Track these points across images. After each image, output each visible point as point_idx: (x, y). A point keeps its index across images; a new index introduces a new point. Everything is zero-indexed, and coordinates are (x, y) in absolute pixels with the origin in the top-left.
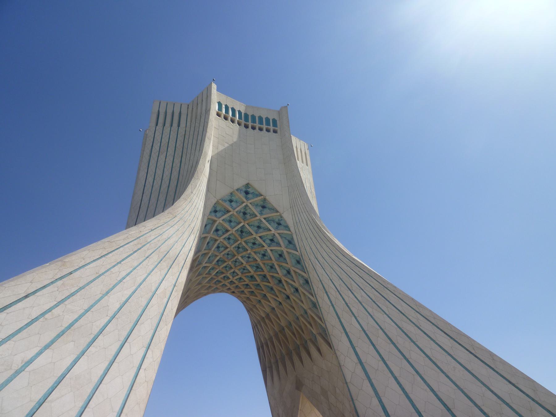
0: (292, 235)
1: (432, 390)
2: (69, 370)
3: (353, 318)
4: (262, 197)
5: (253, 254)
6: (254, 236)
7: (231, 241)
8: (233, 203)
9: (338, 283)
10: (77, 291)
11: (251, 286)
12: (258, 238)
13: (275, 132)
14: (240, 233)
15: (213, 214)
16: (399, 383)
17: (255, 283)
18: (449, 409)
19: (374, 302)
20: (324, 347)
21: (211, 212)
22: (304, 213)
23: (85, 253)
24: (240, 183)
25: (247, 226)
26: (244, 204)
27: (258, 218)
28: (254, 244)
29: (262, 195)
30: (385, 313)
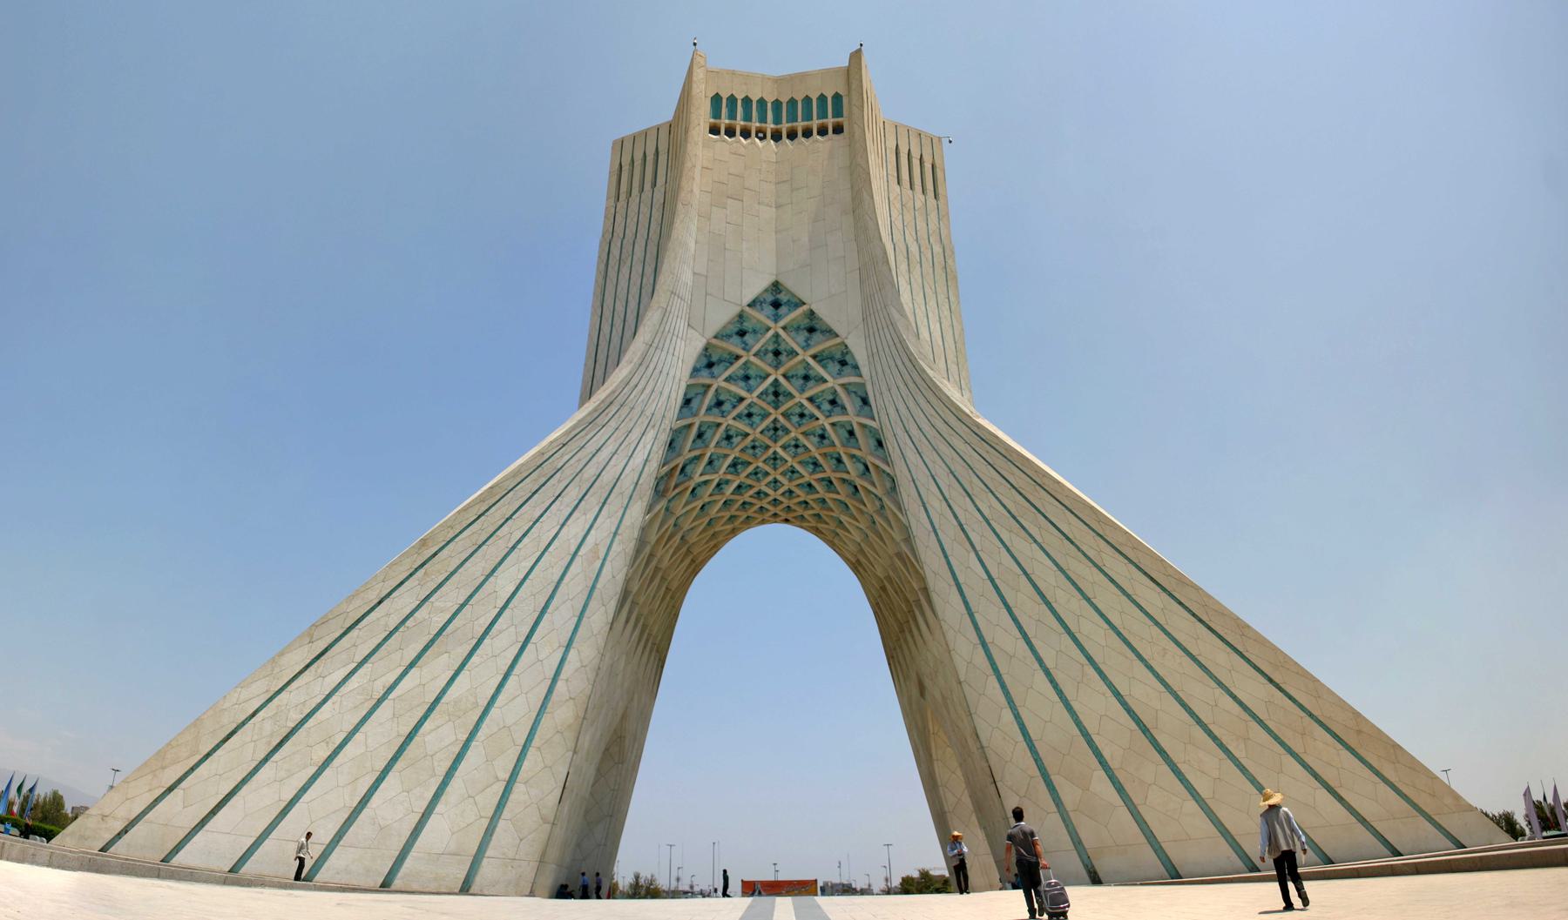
0: (863, 385)
1: (1117, 694)
3: (973, 555)
5: (801, 437)
6: (796, 400)
7: (756, 419)
9: (945, 480)
12: (806, 403)
14: (771, 398)
15: (705, 372)
18: (1145, 730)
21: (695, 371)
25: (782, 380)
26: (771, 333)
27: (799, 358)
28: (802, 415)
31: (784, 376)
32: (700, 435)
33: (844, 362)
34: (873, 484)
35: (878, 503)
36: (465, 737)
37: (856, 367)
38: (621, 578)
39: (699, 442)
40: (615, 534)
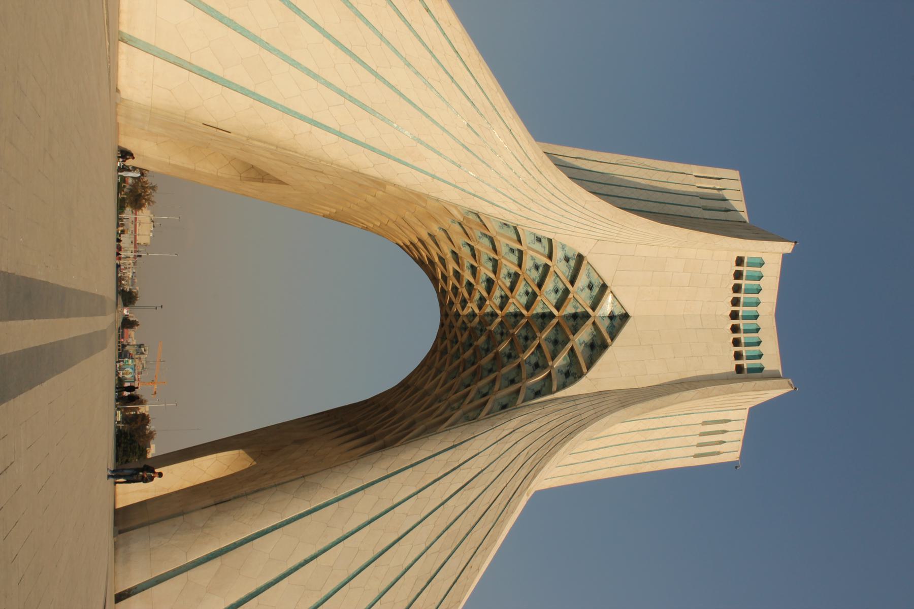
0: (550, 392)
2: (305, 17)
3: (414, 490)
4: (609, 341)
8: (587, 290)
10: (405, 21)
11: (456, 347)
12: (536, 342)
13: (739, 369)
16: (306, 562)
17: (461, 351)
19: (447, 528)
21: (563, 247)
22: (593, 412)
25: (555, 321)
27: (571, 337)
30: (428, 548)
31: (558, 323)
32: (512, 250)
34: (471, 402)
35: (456, 405)
37: (564, 386)
38: (397, 181)
39: (507, 250)
40: (433, 177)
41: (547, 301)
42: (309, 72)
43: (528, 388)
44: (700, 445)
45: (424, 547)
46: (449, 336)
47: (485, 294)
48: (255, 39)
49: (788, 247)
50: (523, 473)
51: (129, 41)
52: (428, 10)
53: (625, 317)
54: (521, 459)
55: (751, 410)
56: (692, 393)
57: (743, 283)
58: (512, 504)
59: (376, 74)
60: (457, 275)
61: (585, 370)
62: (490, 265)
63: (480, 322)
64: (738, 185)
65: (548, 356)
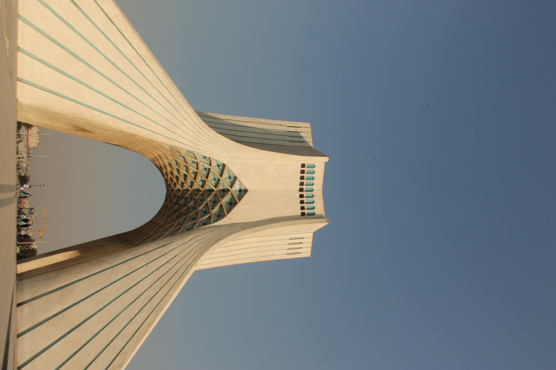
0: (210, 223)
3: (145, 263)
8: (228, 179)
11: (171, 204)
12: (205, 202)
13: (303, 214)
16: (98, 291)
18: (78, 326)
20: (125, 248)
21: (216, 161)
23: (161, 71)
24: (247, 185)
25: (214, 193)
28: (202, 200)
29: (240, 200)
32: (194, 162)
33: (221, 216)
36: (78, 78)
37: (217, 221)
40: (154, 132)
41: (210, 185)
42: (98, 92)
43: (201, 222)
44: (289, 249)
45: (148, 287)
46: (169, 200)
47: (184, 181)
48: (74, 79)
49: (326, 159)
50: (194, 257)
51: (24, 52)
52: (148, 65)
53: (246, 191)
54: (194, 251)
55: (315, 233)
56: (277, 224)
57: (305, 175)
58: (188, 269)
59: (126, 92)
60: (172, 173)
61: (226, 214)
62: (185, 168)
63: (182, 194)
64: (309, 130)
65: (210, 208)
